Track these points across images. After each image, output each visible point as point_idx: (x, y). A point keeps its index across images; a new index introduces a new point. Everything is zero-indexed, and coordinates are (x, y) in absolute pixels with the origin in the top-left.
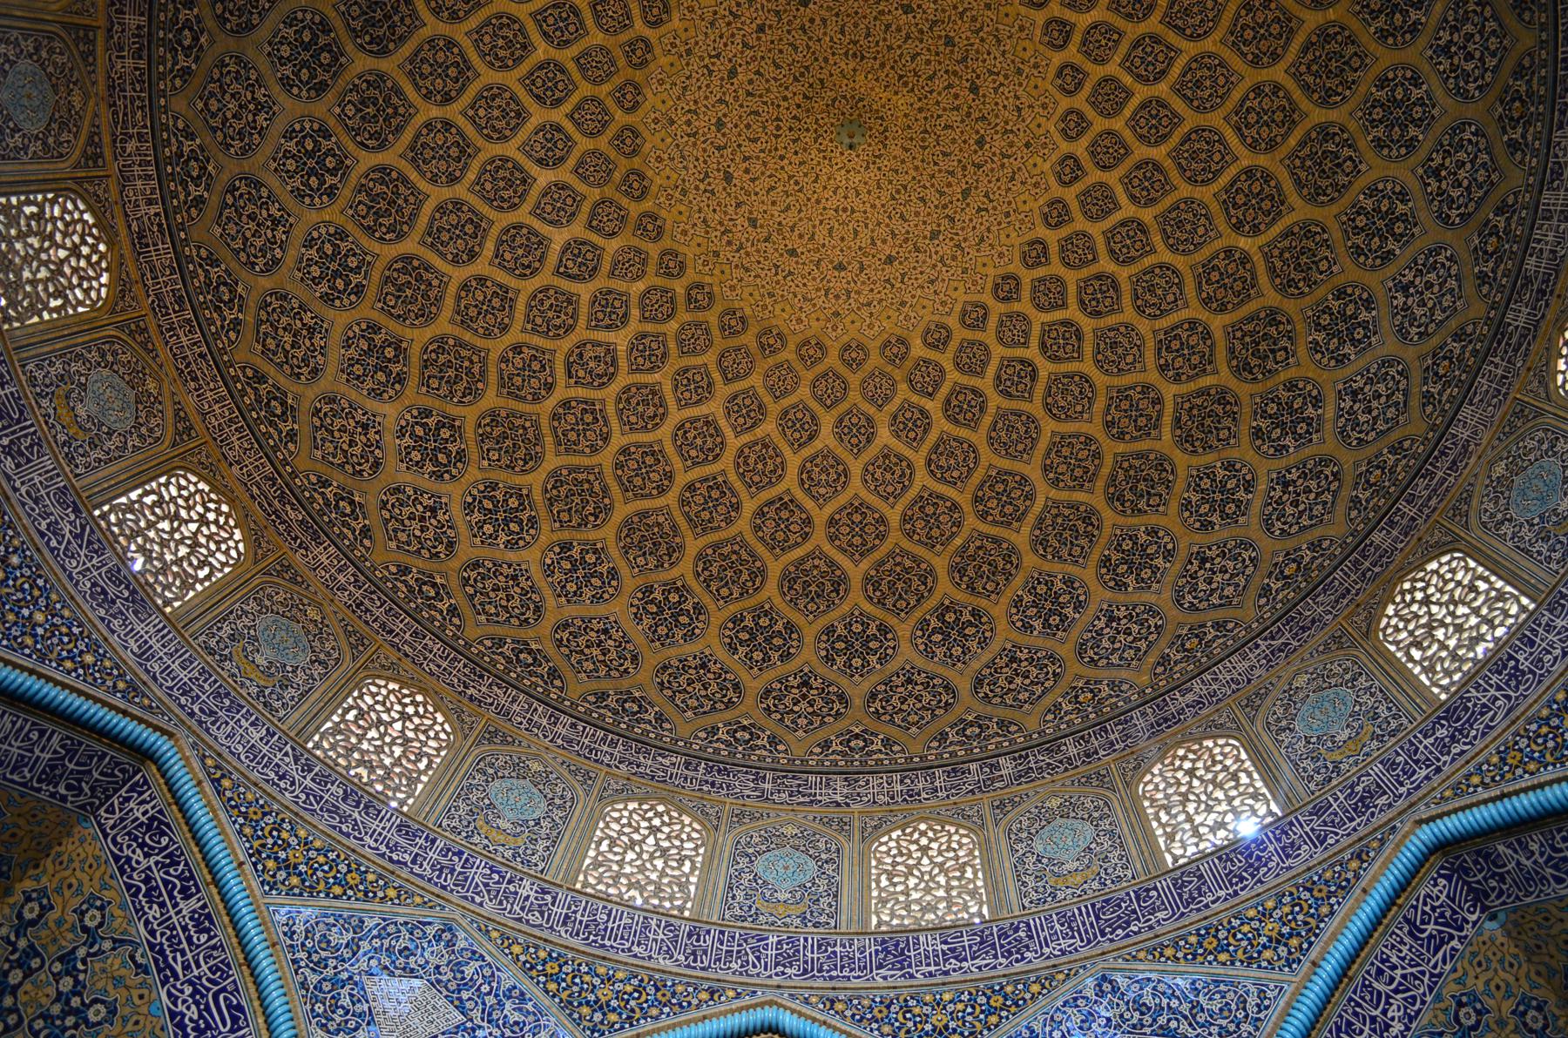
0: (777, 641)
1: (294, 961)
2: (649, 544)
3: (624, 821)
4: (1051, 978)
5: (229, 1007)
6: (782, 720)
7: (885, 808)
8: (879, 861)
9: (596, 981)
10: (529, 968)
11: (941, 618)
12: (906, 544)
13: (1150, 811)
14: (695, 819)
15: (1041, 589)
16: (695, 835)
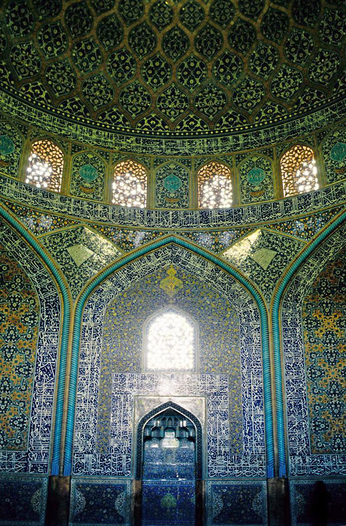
0: (162, 73)
1: (49, 251)
2: (110, 34)
3: (121, 171)
4: (247, 230)
5: (37, 264)
6: (166, 113)
7: (201, 156)
8: (201, 180)
9: (125, 235)
10: (107, 235)
11: (224, 61)
12: (211, 22)
13: (282, 171)
14: (143, 166)
15: (262, 52)
16: (143, 173)
